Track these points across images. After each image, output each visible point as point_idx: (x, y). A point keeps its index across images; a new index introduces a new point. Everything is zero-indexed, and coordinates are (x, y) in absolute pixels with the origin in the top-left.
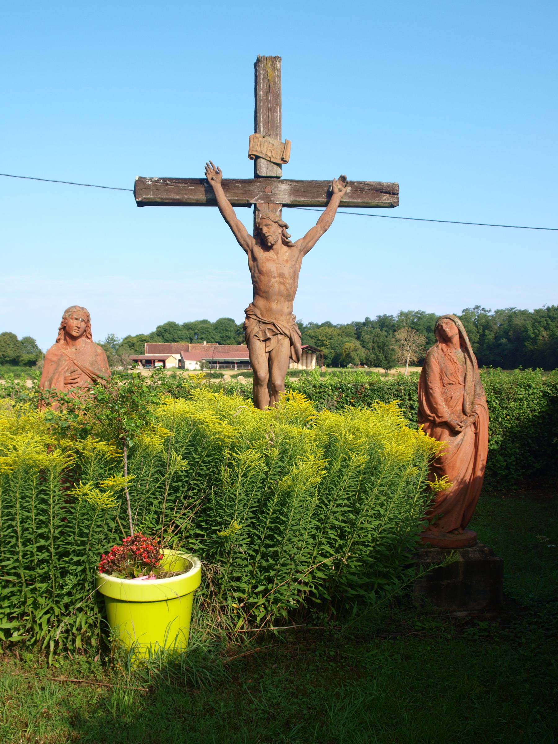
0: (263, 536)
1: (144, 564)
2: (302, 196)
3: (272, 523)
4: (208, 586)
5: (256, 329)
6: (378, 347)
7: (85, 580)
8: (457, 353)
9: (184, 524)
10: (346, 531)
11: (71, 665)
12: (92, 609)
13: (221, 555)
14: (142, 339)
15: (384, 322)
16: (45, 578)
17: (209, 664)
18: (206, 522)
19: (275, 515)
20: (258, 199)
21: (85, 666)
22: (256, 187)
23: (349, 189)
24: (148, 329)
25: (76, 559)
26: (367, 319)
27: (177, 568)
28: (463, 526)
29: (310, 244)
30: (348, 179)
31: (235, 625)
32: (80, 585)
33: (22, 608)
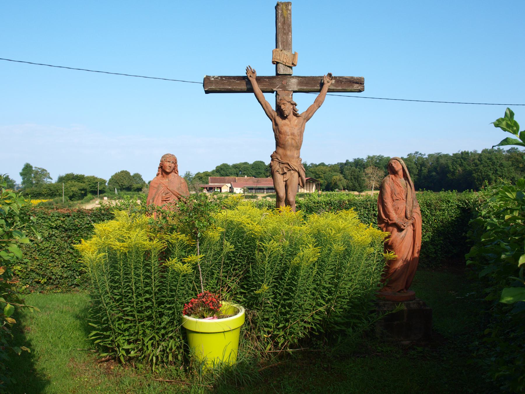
0: (282, 294)
1: (210, 310)
2: (305, 86)
3: (287, 285)
4: (249, 324)
5: (278, 167)
6: (355, 178)
7: (174, 319)
8: (401, 181)
9: (233, 286)
10: (332, 290)
11: (166, 372)
12: (179, 337)
13: (257, 305)
14: (207, 174)
15: (358, 163)
16: (150, 318)
17: (250, 371)
18: (247, 285)
19: (289, 281)
20: (278, 88)
21: (174, 372)
22: (277, 81)
23: (333, 81)
24: (211, 168)
25: (168, 306)
26: (347, 161)
27: (230, 312)
28: (407, 288)
29: (310, 115)
30: (333, 75)
31: (265, 348)
32: (171, 323)
33: (136, 336)
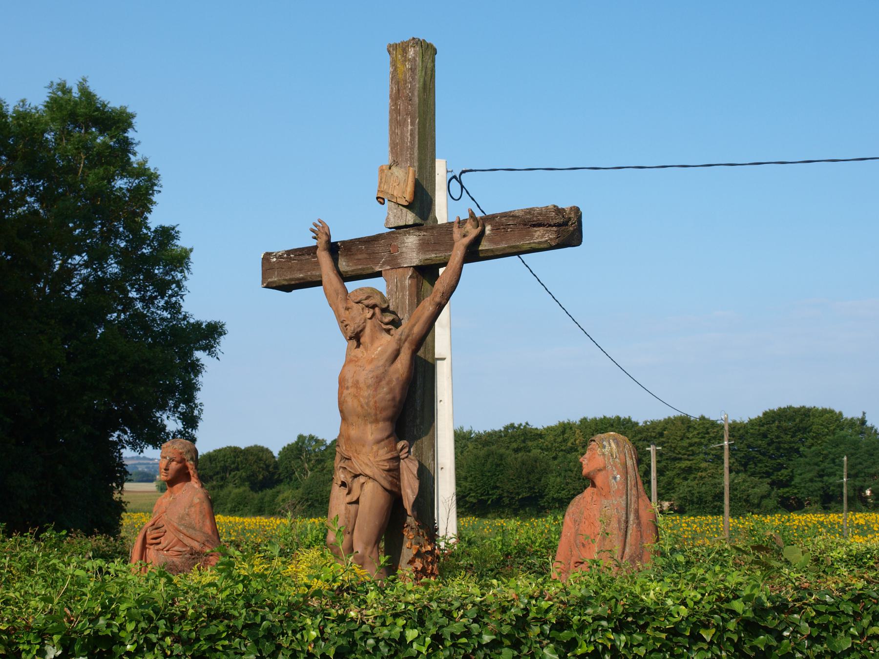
20: (384, 264)
